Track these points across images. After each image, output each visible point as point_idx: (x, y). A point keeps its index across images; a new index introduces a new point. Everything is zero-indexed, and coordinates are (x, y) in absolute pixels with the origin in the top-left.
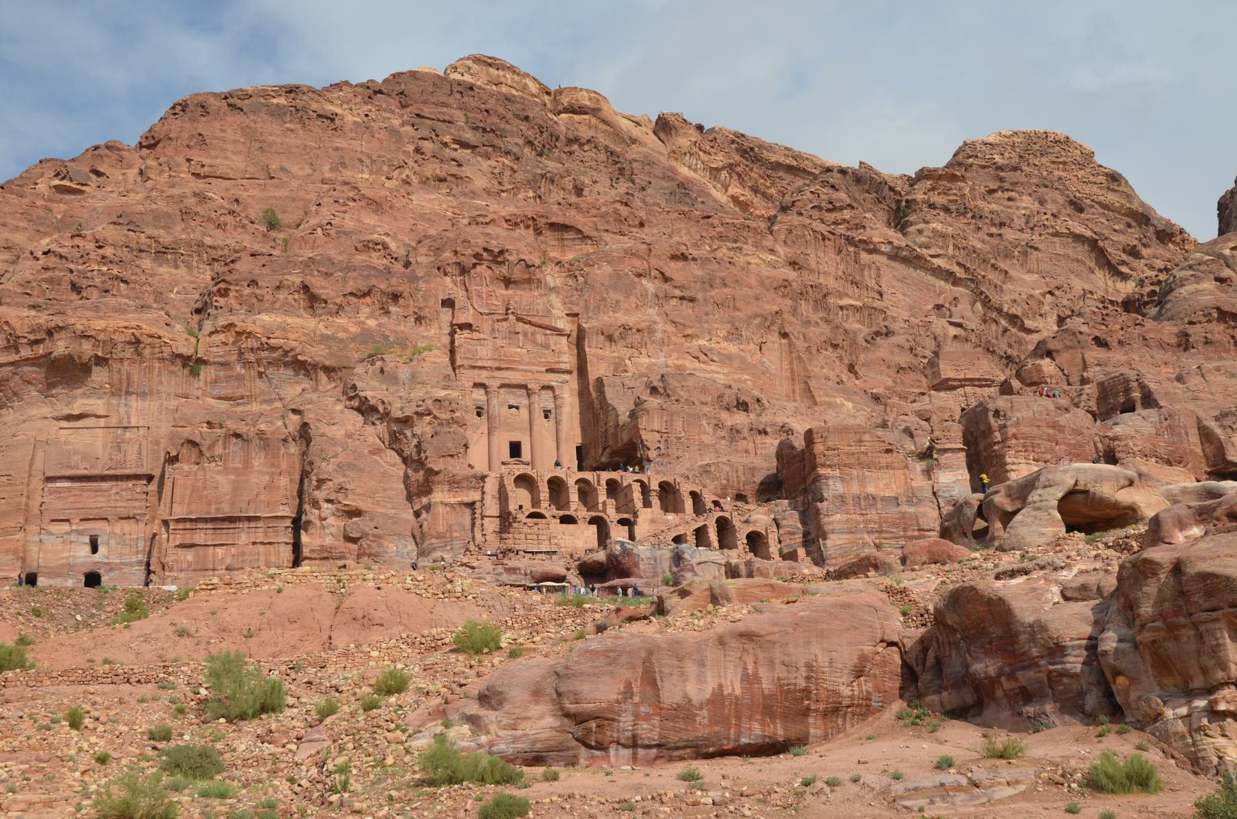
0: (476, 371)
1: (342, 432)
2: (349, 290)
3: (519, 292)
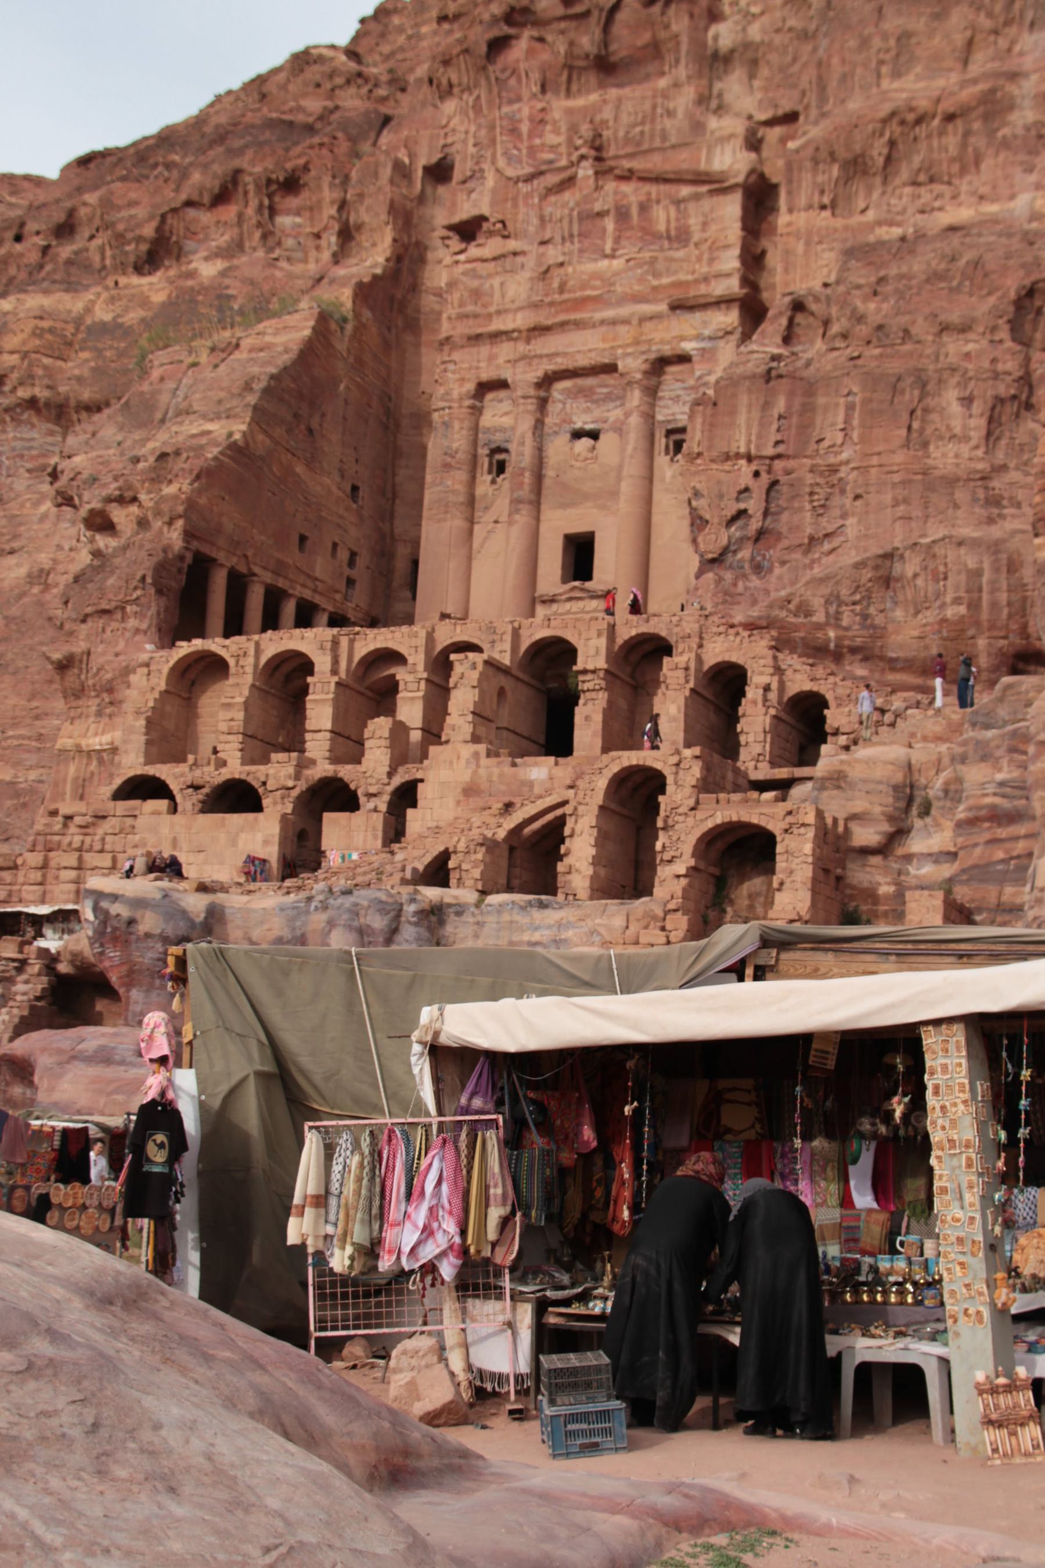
0: (485, 350)
1: (23, 571)
2: (183, 197)
3: (613, 93)
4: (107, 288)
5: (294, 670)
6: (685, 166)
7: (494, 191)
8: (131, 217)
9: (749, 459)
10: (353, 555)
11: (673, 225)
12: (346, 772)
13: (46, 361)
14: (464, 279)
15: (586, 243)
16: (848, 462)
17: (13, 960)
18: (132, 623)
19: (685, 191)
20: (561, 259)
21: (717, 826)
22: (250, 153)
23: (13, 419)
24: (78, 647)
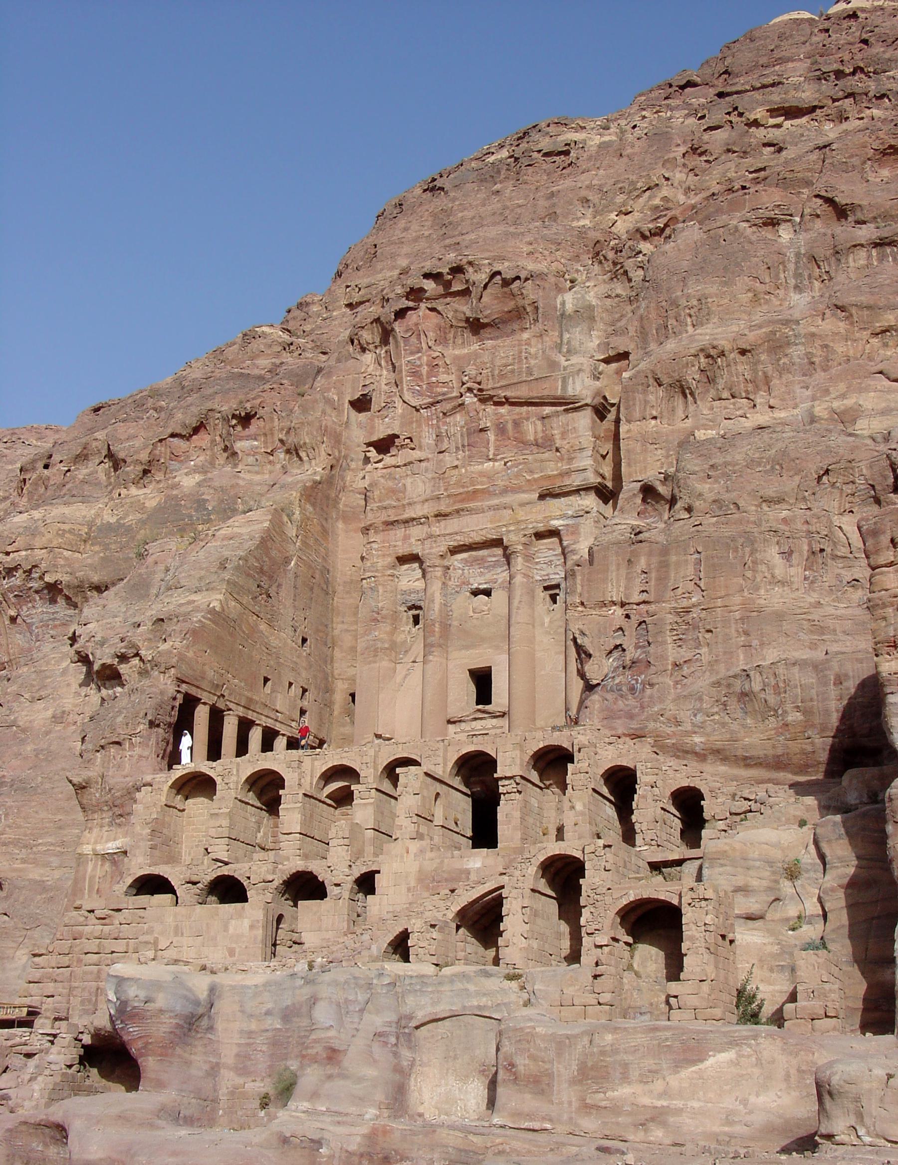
0: (400, 532)
1: (49, 713)
2: (170, 431)
3: (489, 343)
4: (112, 499)
5: (268, 784)
6: (546, 393)
7: (403, 416)
8: (133, 446)
9: (623, 605)
10: (305, 691)
11: (540, 435)
12: (316, 867)
13: (66, 553)
14: (382, 480)
15: (474, 450)
16: (699, 604)
17: (48, 1035)
18: (138, 751)
19: (547, 410)
20: (456, 463)
21: (631, 902)
22: (218, 398)
23: (41, 598)
24: (92, 773)
